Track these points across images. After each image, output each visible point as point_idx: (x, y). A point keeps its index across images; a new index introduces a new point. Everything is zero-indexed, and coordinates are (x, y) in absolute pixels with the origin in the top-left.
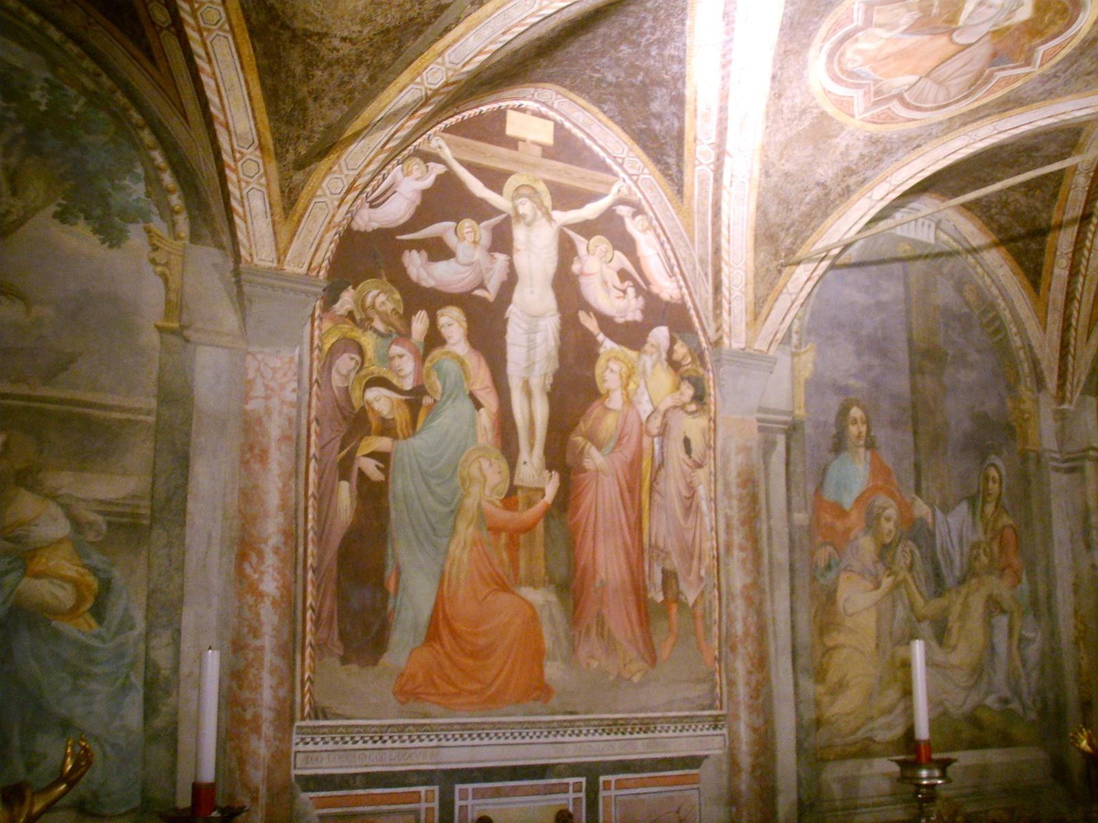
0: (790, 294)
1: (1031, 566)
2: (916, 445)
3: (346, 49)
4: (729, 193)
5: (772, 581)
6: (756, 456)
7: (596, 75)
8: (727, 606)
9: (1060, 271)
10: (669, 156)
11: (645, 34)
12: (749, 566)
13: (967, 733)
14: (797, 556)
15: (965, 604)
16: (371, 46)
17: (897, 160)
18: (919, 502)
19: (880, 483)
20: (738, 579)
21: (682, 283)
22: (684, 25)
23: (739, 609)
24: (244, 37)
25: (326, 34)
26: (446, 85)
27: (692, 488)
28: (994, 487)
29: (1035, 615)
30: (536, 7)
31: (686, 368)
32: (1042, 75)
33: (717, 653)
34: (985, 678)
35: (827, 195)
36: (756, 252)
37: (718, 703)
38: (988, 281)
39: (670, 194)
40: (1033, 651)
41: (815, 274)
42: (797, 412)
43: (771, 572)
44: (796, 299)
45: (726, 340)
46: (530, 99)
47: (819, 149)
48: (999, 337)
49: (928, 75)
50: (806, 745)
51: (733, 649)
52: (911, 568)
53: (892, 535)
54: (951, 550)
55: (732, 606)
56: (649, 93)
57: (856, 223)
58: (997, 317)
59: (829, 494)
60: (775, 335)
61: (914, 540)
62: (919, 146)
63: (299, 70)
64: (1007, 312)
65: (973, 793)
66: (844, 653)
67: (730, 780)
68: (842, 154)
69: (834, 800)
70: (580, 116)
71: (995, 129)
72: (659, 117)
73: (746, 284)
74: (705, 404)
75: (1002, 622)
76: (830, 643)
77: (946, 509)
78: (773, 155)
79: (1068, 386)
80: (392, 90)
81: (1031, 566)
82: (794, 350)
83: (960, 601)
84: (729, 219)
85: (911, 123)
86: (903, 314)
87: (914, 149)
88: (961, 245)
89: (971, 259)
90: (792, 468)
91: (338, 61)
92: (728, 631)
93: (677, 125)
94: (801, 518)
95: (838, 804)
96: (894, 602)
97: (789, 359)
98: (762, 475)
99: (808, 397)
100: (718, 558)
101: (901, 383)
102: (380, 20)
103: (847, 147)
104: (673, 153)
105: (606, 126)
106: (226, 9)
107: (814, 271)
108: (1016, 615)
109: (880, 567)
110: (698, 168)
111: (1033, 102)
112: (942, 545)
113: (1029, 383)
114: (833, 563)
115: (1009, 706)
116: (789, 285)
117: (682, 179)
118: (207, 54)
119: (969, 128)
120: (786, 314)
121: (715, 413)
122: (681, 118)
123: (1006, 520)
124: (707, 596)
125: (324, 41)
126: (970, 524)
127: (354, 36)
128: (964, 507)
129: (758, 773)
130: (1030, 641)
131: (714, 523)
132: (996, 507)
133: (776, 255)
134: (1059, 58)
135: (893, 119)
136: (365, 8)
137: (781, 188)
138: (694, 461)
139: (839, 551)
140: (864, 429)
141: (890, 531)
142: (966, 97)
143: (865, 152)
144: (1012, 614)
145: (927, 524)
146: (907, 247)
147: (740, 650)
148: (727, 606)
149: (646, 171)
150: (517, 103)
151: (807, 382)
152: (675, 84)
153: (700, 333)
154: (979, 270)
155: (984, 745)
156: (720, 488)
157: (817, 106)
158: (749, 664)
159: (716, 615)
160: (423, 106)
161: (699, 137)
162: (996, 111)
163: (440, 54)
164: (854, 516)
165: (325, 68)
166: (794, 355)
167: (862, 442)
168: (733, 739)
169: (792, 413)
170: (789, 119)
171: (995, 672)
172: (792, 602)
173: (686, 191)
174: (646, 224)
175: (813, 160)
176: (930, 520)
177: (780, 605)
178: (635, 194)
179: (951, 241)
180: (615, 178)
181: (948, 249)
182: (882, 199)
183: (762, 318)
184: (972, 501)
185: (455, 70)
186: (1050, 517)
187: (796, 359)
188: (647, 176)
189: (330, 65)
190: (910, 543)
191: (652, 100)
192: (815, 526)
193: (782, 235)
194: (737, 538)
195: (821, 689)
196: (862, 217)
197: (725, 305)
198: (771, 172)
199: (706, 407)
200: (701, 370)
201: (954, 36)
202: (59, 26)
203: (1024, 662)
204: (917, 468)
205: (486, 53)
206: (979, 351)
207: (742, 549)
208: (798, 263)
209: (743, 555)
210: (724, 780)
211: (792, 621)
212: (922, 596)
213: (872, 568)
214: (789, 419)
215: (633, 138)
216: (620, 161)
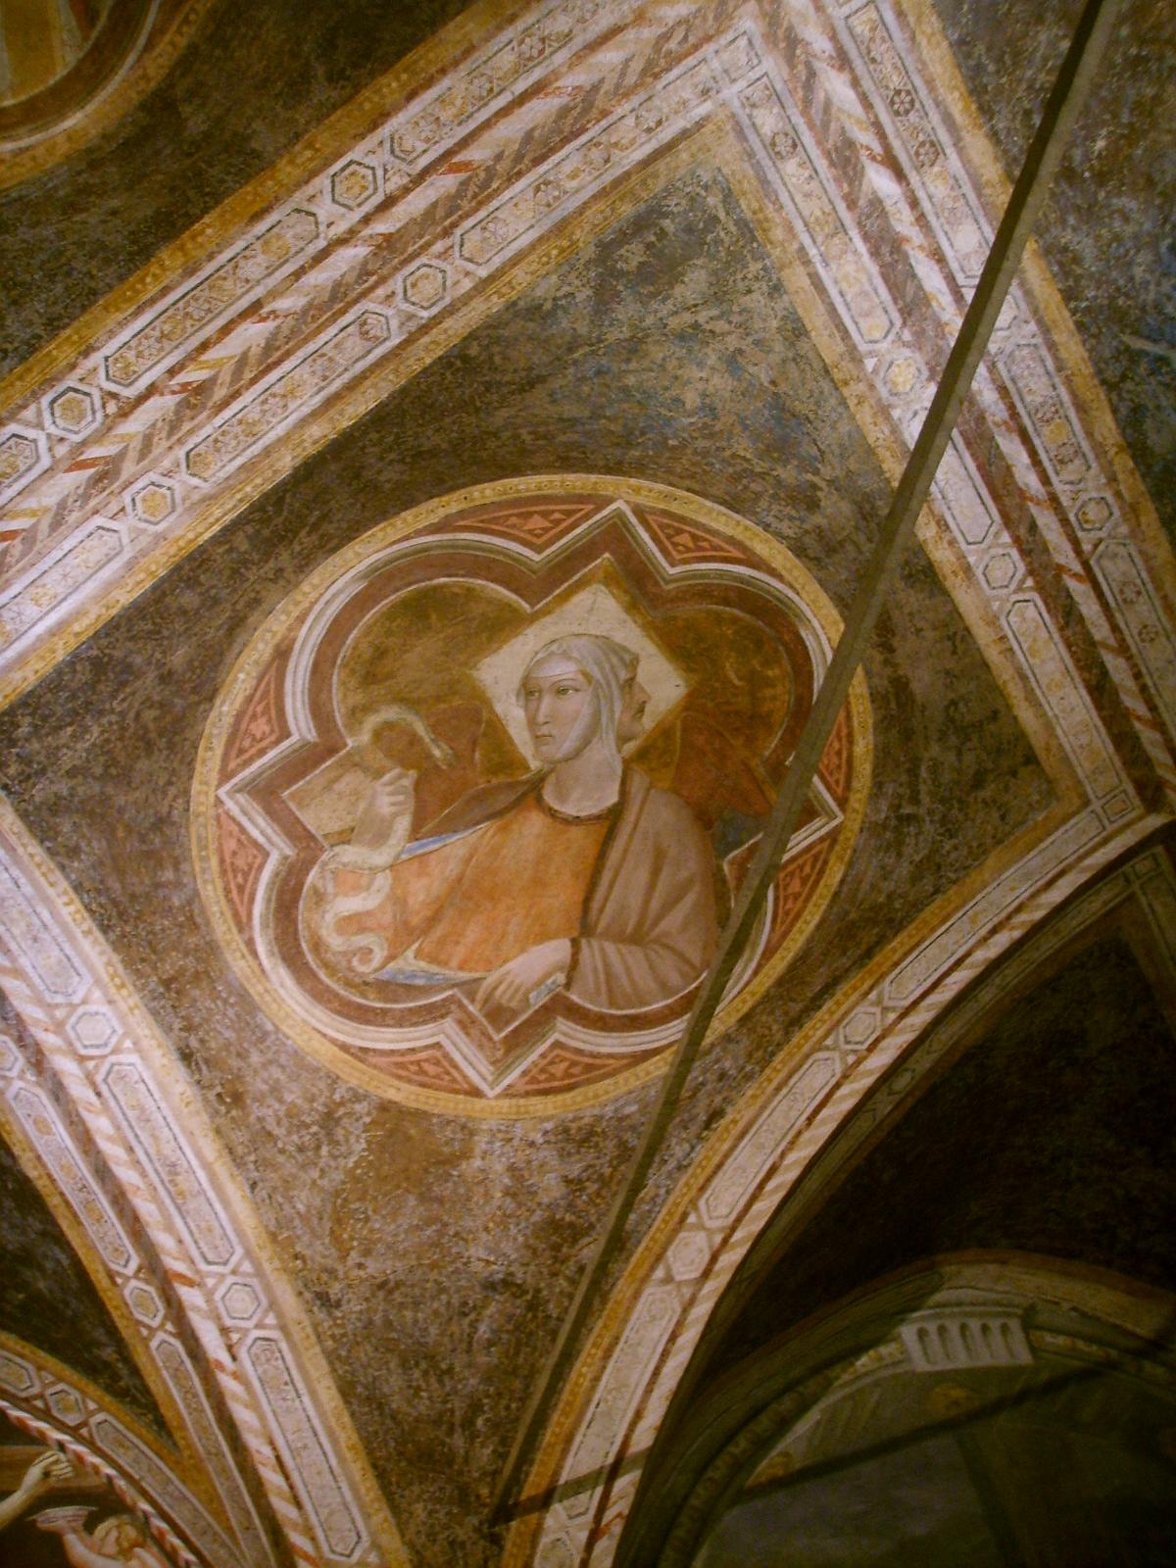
4: (236, 1376)
10: (100, 1345)
17: (681, 1168)
32: (871, 829)
35: (532, 1306)
36: (395, 1509)
39: (150, 1437)
41: (609, 1515)
47: (440, 1201)
49: (584, 928)
57: (665, 1354)
62: (716, 1115)
68: (507, 1192)
71: (885, 1010)
78: (318, 1251)
84: (272, 1443)
85: (641, 1069)
87: (707, 1125)
93: (66, 1262)
103: (512, 1169)
104: (99, 1334)
110: (154, 1344)
111: (918, 906)
117: (146, 1391)
119: (815, 1027)
122: (60, 1240)
133: (464, 1497)
134: (864, 769)
135: (589, 1068)
137: (388, 1324)
142: (736, 950)
143: (575, 1170)
146: (958, 1393)
149: (92, 1406)
157: (357, 1097)
161: (114, 1267)
162: (845, 961)
170: (301, 1149)
173: (168, 1414)
174: (131, 1532)
175: (440, 1233)
178: (96, 1470)
179: (1081, 1344)
180: (33, 1449)
181: (1076, 1364)
182: (706, 1274)
188: (100, 1417)
193: (458, 1441)
196: (673, 1338)
198: (335, 1290)
201: (549, 797)
208: (545, 1501)
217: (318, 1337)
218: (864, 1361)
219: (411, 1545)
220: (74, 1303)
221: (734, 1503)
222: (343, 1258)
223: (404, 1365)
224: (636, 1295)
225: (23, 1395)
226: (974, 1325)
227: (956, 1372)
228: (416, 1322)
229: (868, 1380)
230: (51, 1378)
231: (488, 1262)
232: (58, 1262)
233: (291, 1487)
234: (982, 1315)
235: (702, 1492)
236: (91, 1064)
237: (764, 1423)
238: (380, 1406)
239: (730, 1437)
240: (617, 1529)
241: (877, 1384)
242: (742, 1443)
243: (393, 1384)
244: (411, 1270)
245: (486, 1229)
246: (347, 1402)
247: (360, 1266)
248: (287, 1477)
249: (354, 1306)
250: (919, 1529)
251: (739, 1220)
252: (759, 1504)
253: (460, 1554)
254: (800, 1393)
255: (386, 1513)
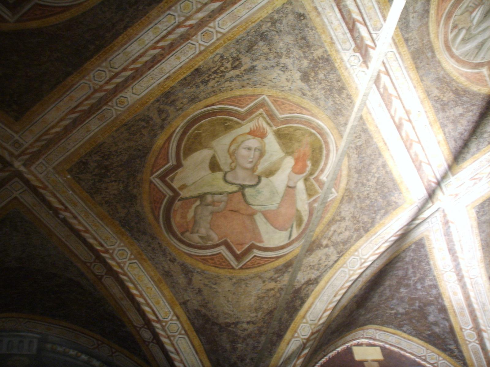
3: (251, 328)
7: (393, 312)
10: (450, 345)
11: (411, 277)
16: (264, 323)
22: (429, 265)
24: (193, 335)
25: (238, 322)
26: (313, 334)
30: (347, 276)
46: (362, 338)
56: (425, 311)
63: (228, 346)
70: (392, 339)
72: (436, 324)
80: (283, 344)
91: (249, 336)
93: (447, 324)
102: (265, 307)
104: (451, 342)
105: (409, 340)
106: (181, 322)
110: (470, 346)
117: (463, 356)
118: (176, 350)
122: (448, 320)
125: (238, 326)
127: (254, 319)
136: (255, 302)
150: (355, 342)
152: (437, 301)
160: (303, 349)
161: (463, 327)
163: (304, 317)
165: (243, 342)
185: (315, 324)
188: (443, 361)
189: (244, 339)
191: (429, 315)
202: (98, 358)
205: (328, 310)
215: (426, 342)
216: (423, 358)
220: (446, 335)
225: (419, 355)
230: (430, 352)
232: (445, 325)
236: (472, 280)
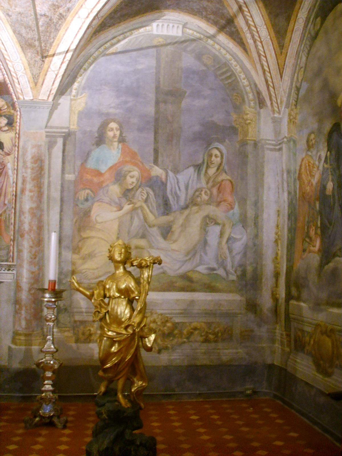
0: (54, 71)
1: (243, 201)
2: (155, 139)
5: (48, 206)
6: (44, 149)
8: (20, 217)
9: (250, 41)
12: (34, 199)
13: (180, 283)
14: (65, 194)
15: (187, 219)
18: (156, 167)
19: (128, 159)
20: (27, 204)
21: (5, 72)
23: (27, 219)
27: (4, 164)
28: (216, 160)
29: (243, 226)
31: (3, 111)
33: (12, 237)
34: (198, 256)
35: (50, 20)
36: (25, 54)
37: (11, 259)
38: (224, 52)
40: (238, 246)
41: (65, 60)
42: (72, 127)
43: (48, 202)
44: (58, 73)
45: (21, 97)
48: (230, 81)
50: (64, 282)
51: (22, 236)
52: (146, 201)
53: (134, 185)
54: (178, 192)
55: (23, 217)
58: (230, 70)
59: (91, 164)
60: (50, 91)
61: (151, 187)
64: (238, 67)
65: (181, 313)
66: (95, 240)
67: (15, 294)
69: (81, 308)
73: (25, 69)
74: (13, 126)
75: (218, 229)
76: (84, 235)
77: (176, 171)
79: (275, 104)
81: (243, 201)
82: (72, 97)
83: (184, 217)
86: (155, 74)
88: (203, 34)
89: (210, 42)
90: (66, 153)
92: (19, 228)
94: (70, 177)
95: (84, 310)
96: (132, 218)
97: (69, 102)
98: (47, 157)
99: (80, 118)
100: (16, 196)
101: (151, 110)
107: (64, 58)
108: (227, 226)
109: (124, 200)
112: (171, 191)
113: (252, 104)
114: (89, 198)
115: (215, 272)
116: (51, 66)
120: (54, 81)
121: (19, 130)
123: (224, 176)
124: (7, 211)
126: (195, 178)
128: (191, 170)
129: (33, 291)
130: (236, 240)
131: (15, 180)
132: (218, 169)
138: (5, 152)
139: (95, 193)
140: (118, 133)
141: (133, 183)
144: (224, 225)
145: (161, 178)
146: (161, 40)
147: (26, 236)
148: (20, 217)
151: (80, 113)
153: (13, 94)
154: (217, 47)
155: (193, 290)
156: (21, 164)
158: (31, 243)
159: (13, 221)
164: (107, 176)
166: (71, 100)
167: (116, 140)
168: (18, 276)
169: (68, 128)
171: (206, 254)
172: (61, 215)
176: (164, 177)
177: (53, 217)
179: (195, 33)
181: (192, 37)
182: (87, 17)
183: (40, 84)
184: (198, 167)
186: (263, 175)
187: (73, 102)
190: (148, 188)
192: (80, 182)
194: (29, 186)
195: (75, 256)
197: (16, 80)
198: (10, 13)
199: (14, 128)
200: (12, 111)
203: (230, 250)
204: (156, 151)
206: (211, 89)
207: (31, 191)
208: (54, 55)
209: (32, 194)
210: (12, 293)
211: (60, 225)
212: (155, 216)
213: (117, 200)
214: (67, 130)
217: (8, 21)
218: (142, 30)
219: (27, 60)
221: (103, 56)
222: (11, 7)
223: (25, 28)
224: (72, 20)
226: (171, 25)
227: (162, 35)
228: (27, 21)
229: (141, 34)
231: (40, 11)
233: (5, 48)
234: (173, 23)
235: (97, 53)
237: (115, 41)
238: (21, 35)
239: (106, 43)
240: (67, 62)
241: (143, 35)
242: (108, 44)
243: (23, 31)
244: (25, 11)
245: (40, 4)
246: (15, 34)
247: (15, 9)
248: (4, 46)
249: (14, 17)
250: (140, 67)
251: (94, 7)
252: (108, 57)
253: (37, 63)
254: (124, 35)
255: (23, 54)
